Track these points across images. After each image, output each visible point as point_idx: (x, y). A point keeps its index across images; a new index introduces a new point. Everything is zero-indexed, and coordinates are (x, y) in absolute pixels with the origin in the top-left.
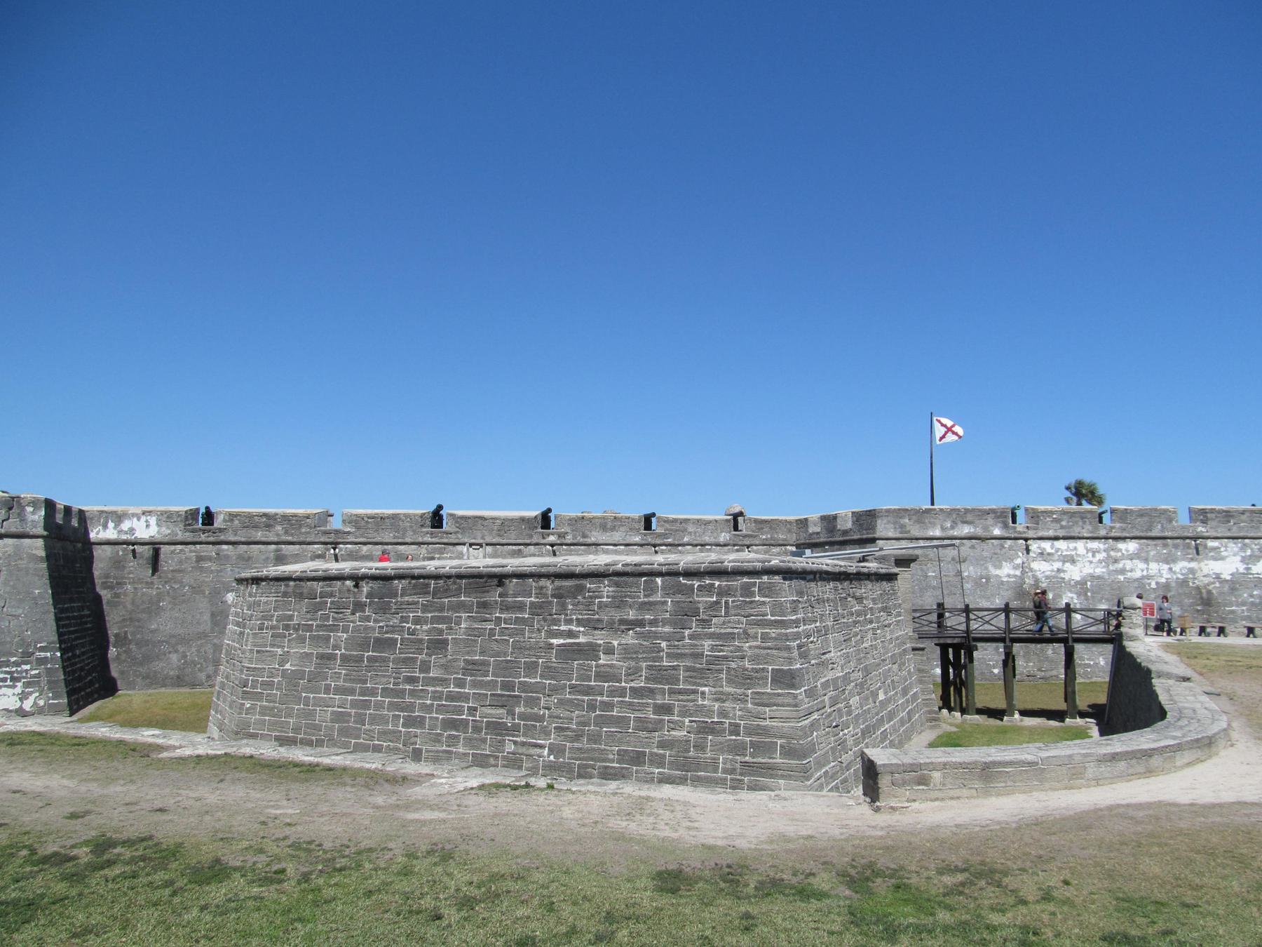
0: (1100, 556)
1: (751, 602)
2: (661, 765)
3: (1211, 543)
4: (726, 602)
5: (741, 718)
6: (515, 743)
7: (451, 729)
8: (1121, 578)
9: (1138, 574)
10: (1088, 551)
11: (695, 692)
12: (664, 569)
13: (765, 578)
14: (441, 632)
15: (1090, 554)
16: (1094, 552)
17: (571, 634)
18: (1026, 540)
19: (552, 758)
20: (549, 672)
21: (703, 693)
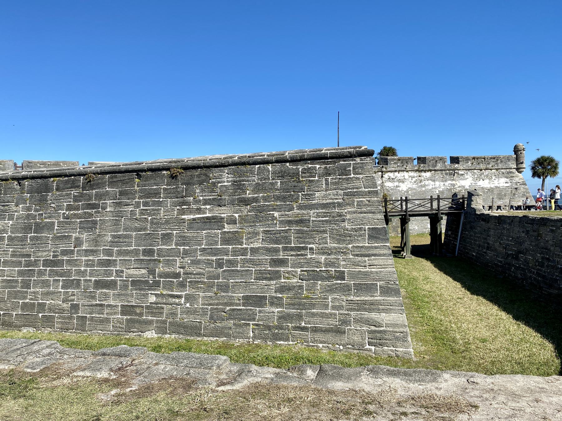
0: (414, 179)
1: (347, 179)
2: (281, 305)
3: (460, 172)
4: (326, 180)
5: (345, 266)
6: (156, 295)
7: (103, 288)
8: (424, 189)
9: (430, 187)
10: (410, 177)
11: (305, 248)
12: (274, 158)
13: (358, 160)
14: (91, 215)
15: (410, 178)
16: (413, 177)
17: (199, 211)
18: (382, 172)
19: (188, 305)
20: (183, 240)
21: (311, 249)
